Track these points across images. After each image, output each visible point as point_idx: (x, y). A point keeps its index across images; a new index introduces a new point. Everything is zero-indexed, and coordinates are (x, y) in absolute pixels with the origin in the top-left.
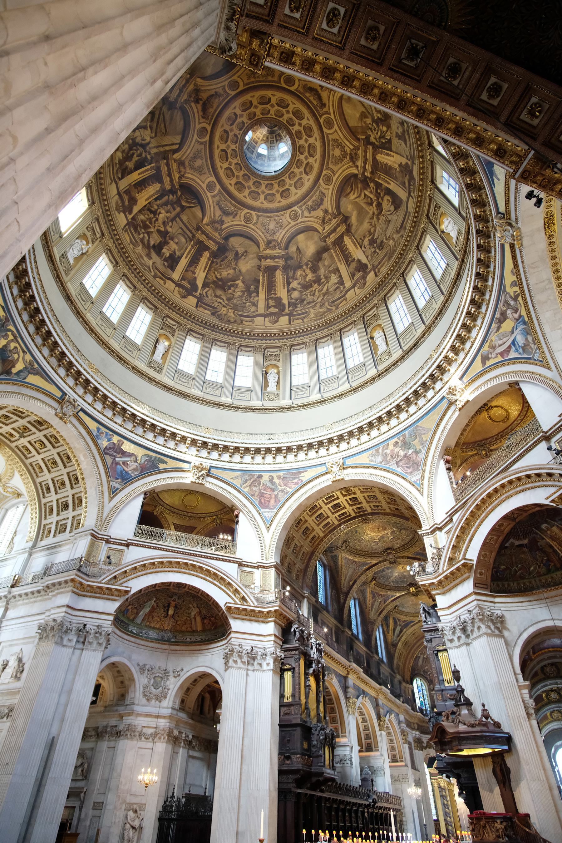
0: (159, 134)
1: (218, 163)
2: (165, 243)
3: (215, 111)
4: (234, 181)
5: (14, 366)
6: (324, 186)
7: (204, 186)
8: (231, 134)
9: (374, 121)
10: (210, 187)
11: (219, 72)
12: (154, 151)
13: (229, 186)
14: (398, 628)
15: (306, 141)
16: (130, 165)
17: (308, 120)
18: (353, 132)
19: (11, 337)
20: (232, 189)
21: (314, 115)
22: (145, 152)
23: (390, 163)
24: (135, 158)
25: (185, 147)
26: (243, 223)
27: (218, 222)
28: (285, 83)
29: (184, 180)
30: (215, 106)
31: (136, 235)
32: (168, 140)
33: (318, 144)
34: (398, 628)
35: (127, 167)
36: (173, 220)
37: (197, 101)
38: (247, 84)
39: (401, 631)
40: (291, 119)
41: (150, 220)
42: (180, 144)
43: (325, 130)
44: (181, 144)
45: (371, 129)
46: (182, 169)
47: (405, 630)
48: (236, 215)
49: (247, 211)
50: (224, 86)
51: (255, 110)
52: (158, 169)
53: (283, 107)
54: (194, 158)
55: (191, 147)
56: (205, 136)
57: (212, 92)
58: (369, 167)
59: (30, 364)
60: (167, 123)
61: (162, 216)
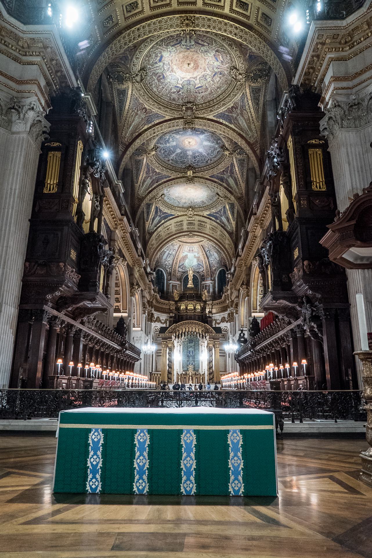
14: (158, 219)
34: (158, 219)
39: (159, 222)
47: (163, 221)
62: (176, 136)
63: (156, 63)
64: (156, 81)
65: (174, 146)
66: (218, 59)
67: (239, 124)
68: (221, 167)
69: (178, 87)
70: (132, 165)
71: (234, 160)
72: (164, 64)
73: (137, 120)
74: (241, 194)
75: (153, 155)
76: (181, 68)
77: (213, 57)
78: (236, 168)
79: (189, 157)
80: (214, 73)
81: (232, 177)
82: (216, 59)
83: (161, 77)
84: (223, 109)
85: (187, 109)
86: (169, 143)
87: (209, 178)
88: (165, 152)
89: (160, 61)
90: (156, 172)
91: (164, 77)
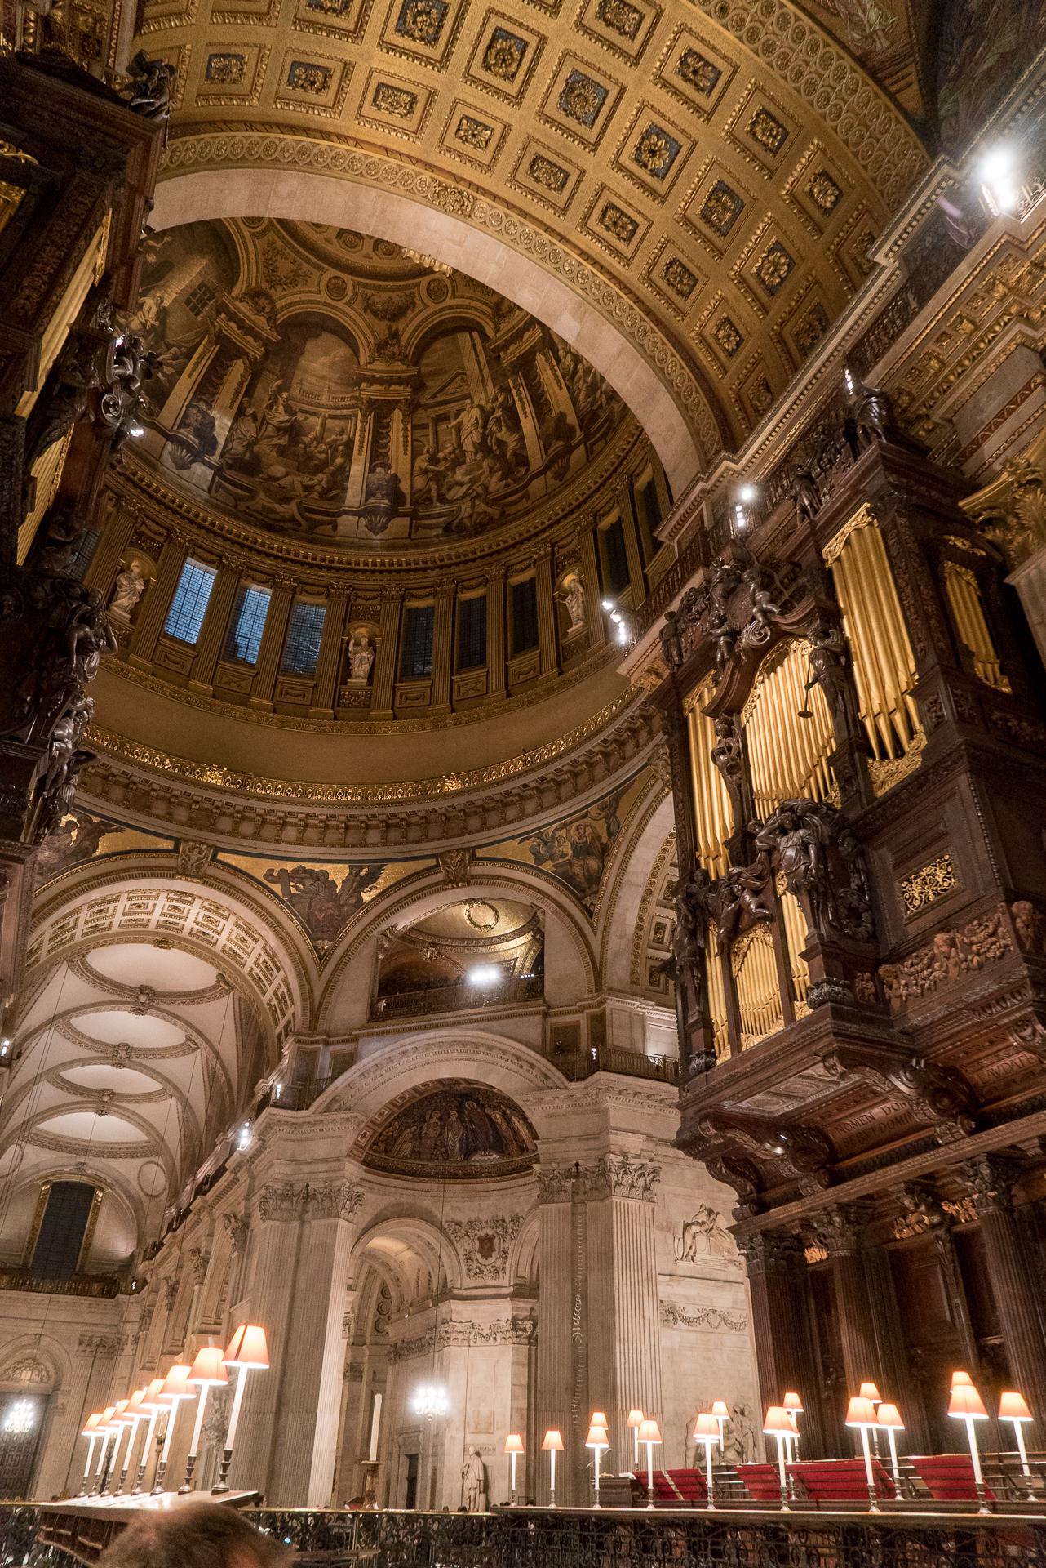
0: (465, 390)
3: (392, 289)
5: (599, 838)
11: (333, 332)
12: (492, 390)
16: (511, 440)
19: (563, 833)
24: (504, 434)
25: (474, 315)
30: (385, 295)
31: (603, 417)
32: (471, 365)
35: (515, 454)
37: (395, 336)
38: (319, 268)
42: (470, 330)
55: (467, 302)
57: (369, 316)
59: (602, 809)
60: (447, 378)
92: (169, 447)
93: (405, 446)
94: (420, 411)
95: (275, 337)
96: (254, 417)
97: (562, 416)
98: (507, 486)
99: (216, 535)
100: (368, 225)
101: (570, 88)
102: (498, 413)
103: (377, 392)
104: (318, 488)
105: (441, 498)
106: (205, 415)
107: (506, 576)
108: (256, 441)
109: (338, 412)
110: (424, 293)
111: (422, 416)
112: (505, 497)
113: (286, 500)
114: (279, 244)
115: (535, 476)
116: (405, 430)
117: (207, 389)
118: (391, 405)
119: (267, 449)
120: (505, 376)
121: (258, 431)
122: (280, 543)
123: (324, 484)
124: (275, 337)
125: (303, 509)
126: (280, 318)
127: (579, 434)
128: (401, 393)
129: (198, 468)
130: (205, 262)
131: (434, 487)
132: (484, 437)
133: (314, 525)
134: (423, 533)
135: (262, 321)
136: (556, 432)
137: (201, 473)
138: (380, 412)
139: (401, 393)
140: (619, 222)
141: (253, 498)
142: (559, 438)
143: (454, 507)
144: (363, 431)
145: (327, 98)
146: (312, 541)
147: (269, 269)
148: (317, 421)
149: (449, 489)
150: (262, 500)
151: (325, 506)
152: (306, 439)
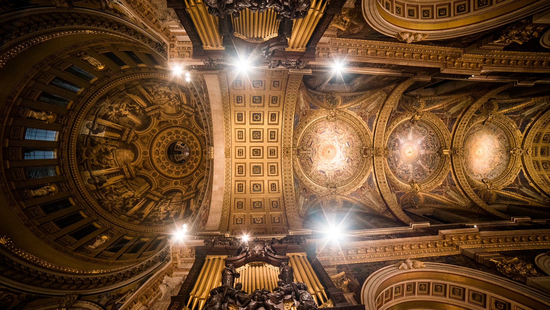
1: (171, 175)
2: (170, 214)
3: (150, 165)
4: (181, 173)
6: (199, 134)
7: (174, 186)
8: (164, 164)
9: (171, 100)
10: (176, 184)
11: (135, 155)
12: (139, 195)
13: (182, 176)
15: (181, 135)
16: (130, 206)
17: (173, 130)
18: (179, 112)
20: (184, 175)
21: (171, 127)
22: (135, 198)
23: (185, 98)
24: (131, 203)
25: (154, 184)
26: (197, 178)
27: (189, 188)
28: (154, 133)
29: (163, 193)
32: (143, 188)
33: (183, 130)
35: (128, 208)
36: (169, 206)
37: (140, 169)
38: (148, 148)
40: (171, 137)
41: (157, 214)
42: (150, 185)
43: (178, 125)
44: (151, 185)
45: (175, 103)
46: (159, 190)
48: (193, 179)
49: (194, 174)
50: (143, 157)
51: (161, 150)
52: (148, 198)
53: (165, 139)
54: (161, 183)
56: (157, 174)
57: (142, 162)
58: (191, 109)
60: (137, 184)
61: (162, 208)
62: (400, 164)
63: (325, 175)
64: (341, 177)
65: (413, 166)
66: (323, 131)
67: (374, 109)
68: (437, 121)
69: (348, 160)
70: (430, 207)
71: (426, 110)
72: (327, 170)
73: (370, 196)
74: (467, 97)
75: (419, 186)
76: (332, 158)
77: (322, 134)
78: (436, 107)
79: (427, 152)
80: (336, 133)
81: (449, 110)
82: (323, 132)
83: (338, 173)
84: (365, 124)
85: (365, 154)
86: (408, 170)
87: (452, 133)
88: (419, 174)
89: (324, 172)
90: (441, 185)
91: (339, 171)
92: (91, 122)
93: (115, 181)
94: (126, 181)
95: (129, 142)
96: (107, 142)
97: (143, 214)
98: (119, 210)
99: (69, 139)
100: (216, 137)
101: (257, 167)
102: (135, 199)
103: (125, 169)
104: (94, 163)
105: (106, 195)
106: (103, 130)
107: (94, 221)
108: (101, 144)
109: (116, 162)
110: (153, 172)
111: (125, 182)
112: (116, 210)
113: (87, 156)
114: (150, 138)
115: (125, 215)
116: (119, 179)
117: (110, 129)
118: (124, 174)
119: (100, 147)
120: (144, 197)
121: (103, 144)
122: (74, 157)
123: (96, 164)
124: (129, 142)
125: (86, 160)
126: (133, 143)
127: (142, 220)
128: (128, 175)
129: (88, 130)
130: (140, 123)
131: (108, 192)
132: (127, 199)
133: (83, 164)
134: (94, 194)
135: (131, 139)
136: (138, 213)
137: (87, 131)
138: (121, 172)
139: (128, 175)
140: (240, 188)
141: (85, 147)
142: (138, 216)
143: (106, 199)
144: (114, 169)
145: (237, 122)
146: (78, 166)
147: (143, 138)
148: (112, 158)
149: (110, 196)
150: (85, 149)
151: (90, 166)
152: (106, 156)
